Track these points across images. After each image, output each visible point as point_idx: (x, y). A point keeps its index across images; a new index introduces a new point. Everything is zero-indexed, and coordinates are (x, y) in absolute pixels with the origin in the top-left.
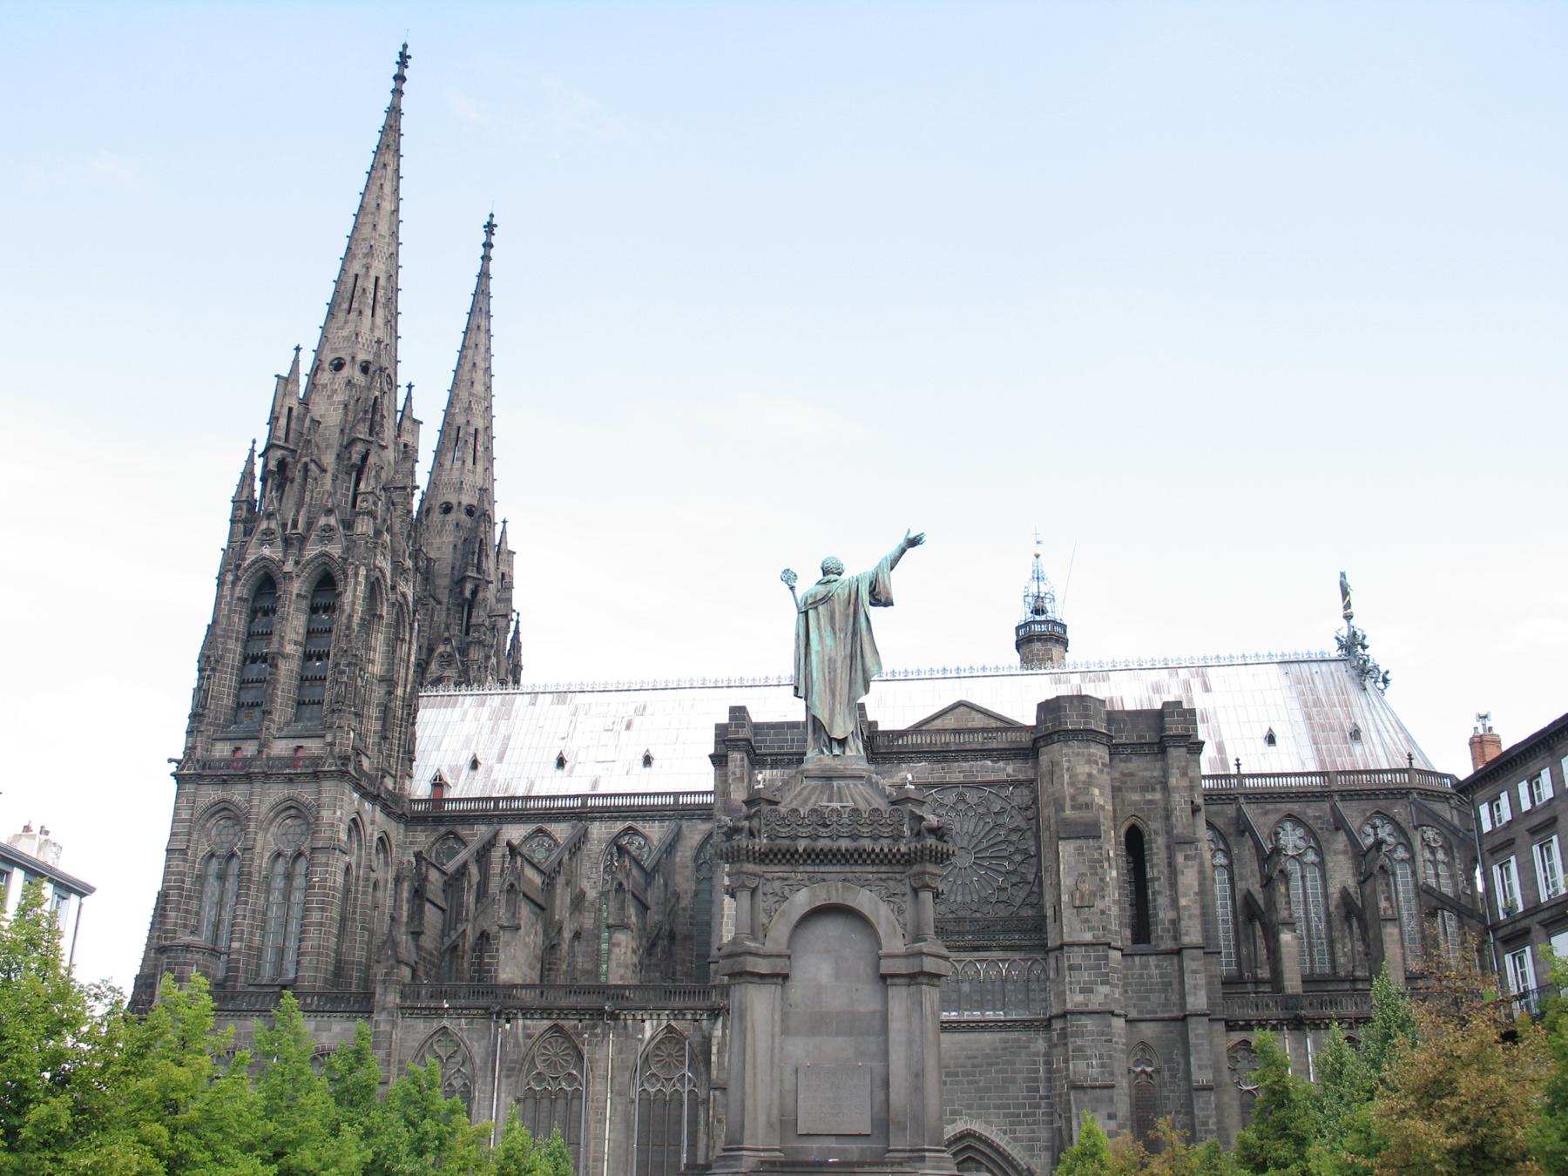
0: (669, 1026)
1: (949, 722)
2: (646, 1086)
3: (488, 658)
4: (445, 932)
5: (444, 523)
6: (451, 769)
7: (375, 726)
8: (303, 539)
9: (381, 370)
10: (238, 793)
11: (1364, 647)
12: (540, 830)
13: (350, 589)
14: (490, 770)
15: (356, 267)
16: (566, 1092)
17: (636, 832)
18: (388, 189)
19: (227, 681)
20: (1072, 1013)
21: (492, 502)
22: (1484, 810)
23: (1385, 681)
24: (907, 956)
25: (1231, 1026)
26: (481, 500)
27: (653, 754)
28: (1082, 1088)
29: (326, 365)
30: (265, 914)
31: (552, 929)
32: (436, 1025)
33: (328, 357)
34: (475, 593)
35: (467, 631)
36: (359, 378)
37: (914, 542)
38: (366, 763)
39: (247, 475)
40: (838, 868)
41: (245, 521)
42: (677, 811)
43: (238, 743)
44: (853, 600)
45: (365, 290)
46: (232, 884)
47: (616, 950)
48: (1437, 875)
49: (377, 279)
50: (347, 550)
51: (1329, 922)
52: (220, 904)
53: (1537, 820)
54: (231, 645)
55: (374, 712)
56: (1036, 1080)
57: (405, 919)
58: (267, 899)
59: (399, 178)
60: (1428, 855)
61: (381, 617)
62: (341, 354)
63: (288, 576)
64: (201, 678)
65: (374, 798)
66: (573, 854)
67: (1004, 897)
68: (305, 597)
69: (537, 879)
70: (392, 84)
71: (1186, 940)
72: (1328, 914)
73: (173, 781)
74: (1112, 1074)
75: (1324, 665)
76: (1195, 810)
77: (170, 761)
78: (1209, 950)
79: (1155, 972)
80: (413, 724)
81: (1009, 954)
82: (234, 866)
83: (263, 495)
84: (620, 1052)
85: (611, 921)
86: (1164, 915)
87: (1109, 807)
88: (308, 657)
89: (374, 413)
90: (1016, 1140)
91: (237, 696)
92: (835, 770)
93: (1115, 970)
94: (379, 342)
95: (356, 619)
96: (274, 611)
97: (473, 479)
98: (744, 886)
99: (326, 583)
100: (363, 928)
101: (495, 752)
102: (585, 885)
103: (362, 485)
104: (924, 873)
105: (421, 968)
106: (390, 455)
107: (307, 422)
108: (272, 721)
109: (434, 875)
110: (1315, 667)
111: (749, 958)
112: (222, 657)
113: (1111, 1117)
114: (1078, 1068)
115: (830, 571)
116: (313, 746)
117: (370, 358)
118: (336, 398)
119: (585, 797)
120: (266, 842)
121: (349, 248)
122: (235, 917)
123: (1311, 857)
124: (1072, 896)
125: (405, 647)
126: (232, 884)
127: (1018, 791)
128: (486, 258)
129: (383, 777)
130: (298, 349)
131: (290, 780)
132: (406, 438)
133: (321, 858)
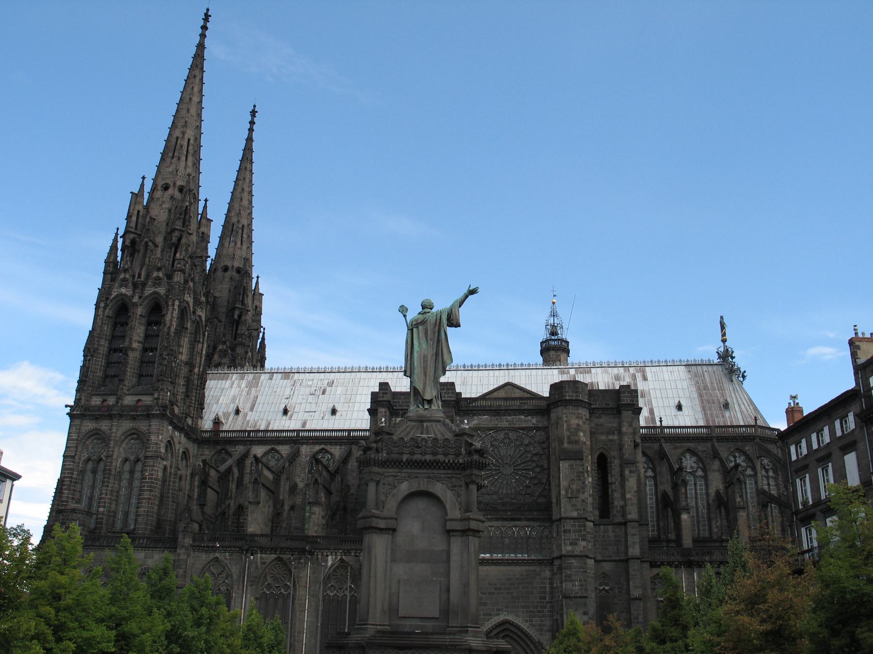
0: (342, 560)
1: (501, 394)
2: (328, 592)
3: (246, 353)
4: (218, 505)
5: (224, 277)
6: (224, 414)
7: (182, 389)
8: (144, 284)
9: (190, 191)
10: (104, 425)
11: (733, 358)
12: (273, 449)
13: (169, 312)
14: (246, 415)
15: (177, 133)
16: (284, 595)
17: (327, 452)
18: (196, 90)
19: (100, 362)
20: (565, 556)
21: (251, 266)
22: (793, 448)
23: (744, 377)
24: (461, 520)
25: (653, 565)
26: (245, 265)
27: (338, 408)
28: (569, 597)
29: (159, 187)
30: (118, 492)
31: (278, 504)
32: (212, 556)
33: (161, 183)
34: (240, 316)
35: (237, 339)
36: (177, 195)
37: (472, 292)
38: (176, 410)
39: (114, 248)
40: (425, 471)
41: (111, 273)
42: (348, 439)
43: (105, 397)
44: (438, 323)
45: (182, 146)
46: (100, 475)
47: (313, 516)
48: (769, 484)
49: (189, 140)
50: (168, 291)
51: (709, 509)
52: (93, 487)
53: (820, 454)
54: (103, 342)
55: (182, 382)
56: (545, 593)
57: (196, 497)
58: (119, 485)
59: (203, 83)
60: (764, 473)
61: (187, 328)
62: (168, 181)
63: (135, 305)
64: (85, 360)
65: (181, 429)
66: (291, 463)
67: (529, 491)
68: (144, 317)
69: (270, 476)
70: (200, 31)
71: (629, 517)
72: (708, 505)
73: (68, 418)
74: (586, 590)
75: (710, 368)
76: (636, 445)
77: (67, 406)
78: (642, 522)
79: (611, 534)
80: (204, 389)
81: (531, 523)
82: (102, 464)
83: (122, 259)
84: (314, 573)
85: (311, 500)
86: (618, 503)
87: (588, 443)
88: (145, 350)
89: (186, 214)
90: (532, 625)
91: (105, 371)
92: (425, 417)
93: (589, 533)
94: (189, 175)
95: (173, 330)
96: (127, 324)
97: (241, 253)
98: (372, 480)
99: (156, 309)
100: (173, 502)
101: (249, 405)
102: (298, 480)
103: (178, 255)
104: (472, 475)
105: (204, 524)
106: (194, 238)
107: (148, 219)
108: (125, 385)
109: (213, 473)
110: (705, 368)
111: (374, 519)
112: (97, 349)
113: (585, 613)
114: (567, 586)
115: (426, 306)
116: (147, 400)
117: (184, 184)
118: (164, 206)
119: (298, 431)
120: (119, 453)
121: (173, 122)
122: (101, 494)
123: (700, 473)
124: (567, 492)
125: (200, 346)
126: (100, 475)
127: (538, 433)
128: (251, 130)
129: (186, 418)
130: (144, 178)
131: (134, 418)
132: (203, 229)
133: (150, 462)
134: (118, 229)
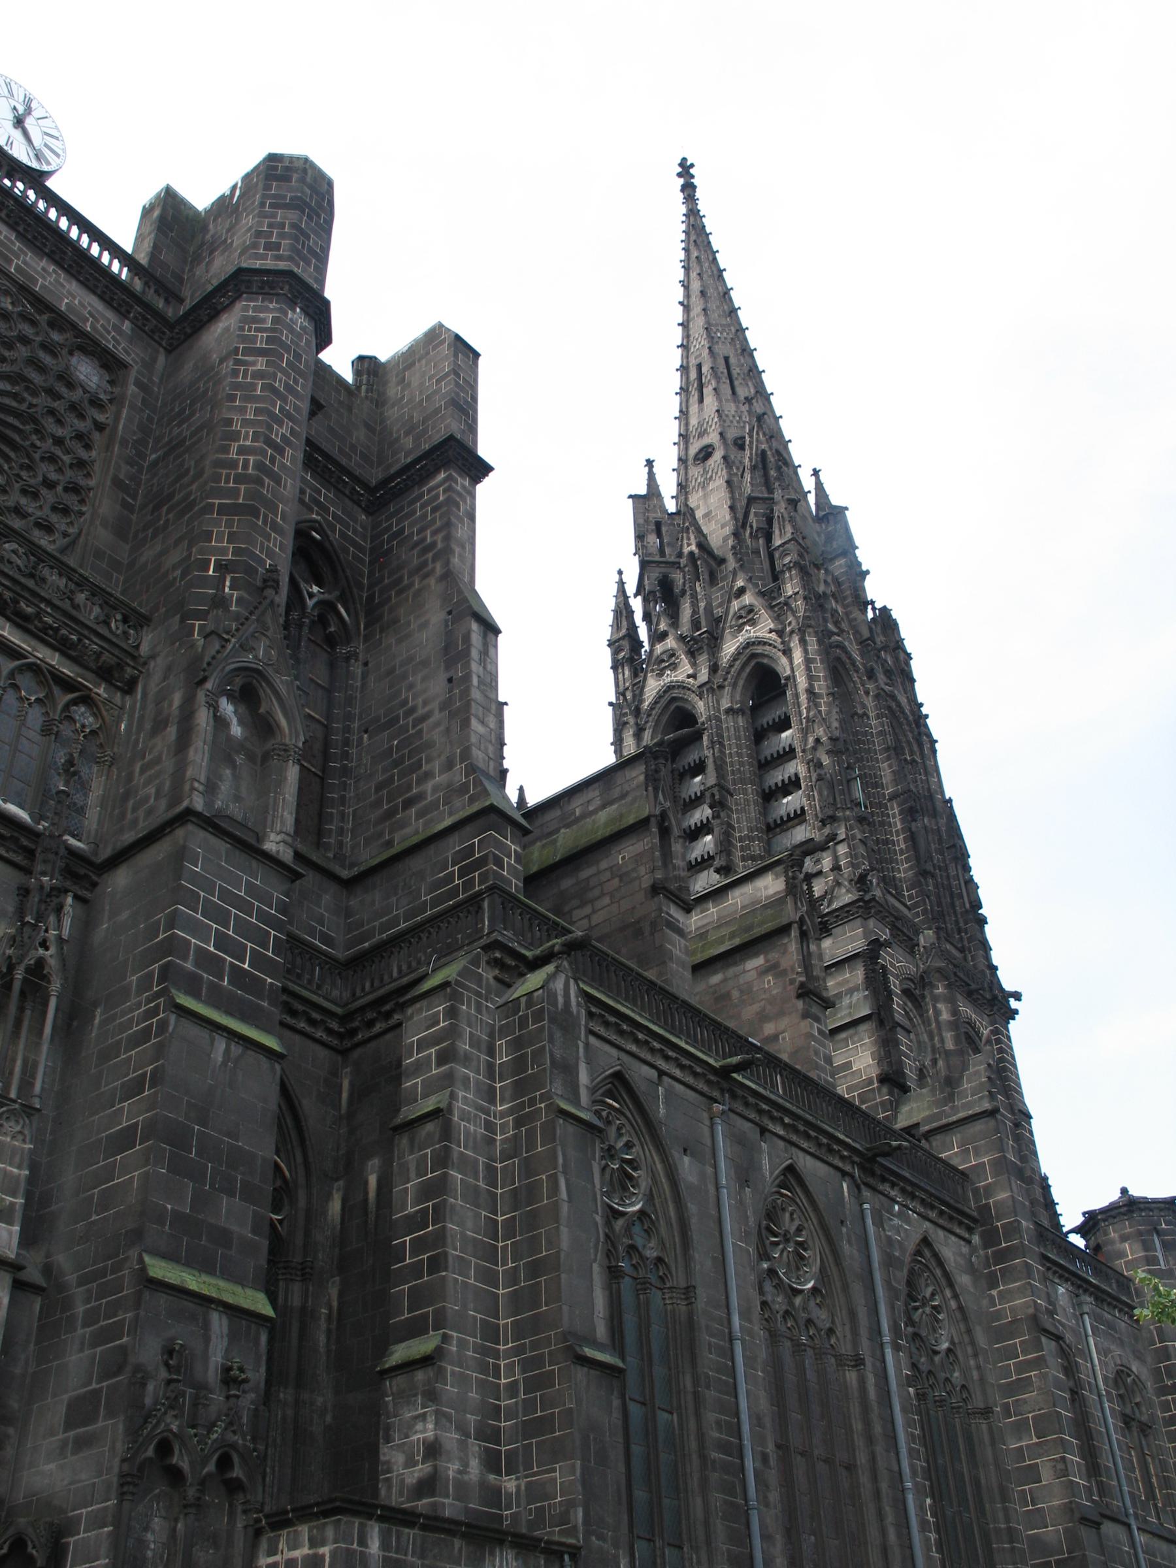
39: (623, 612)
68: (741, 711)
134: (620, 573)
